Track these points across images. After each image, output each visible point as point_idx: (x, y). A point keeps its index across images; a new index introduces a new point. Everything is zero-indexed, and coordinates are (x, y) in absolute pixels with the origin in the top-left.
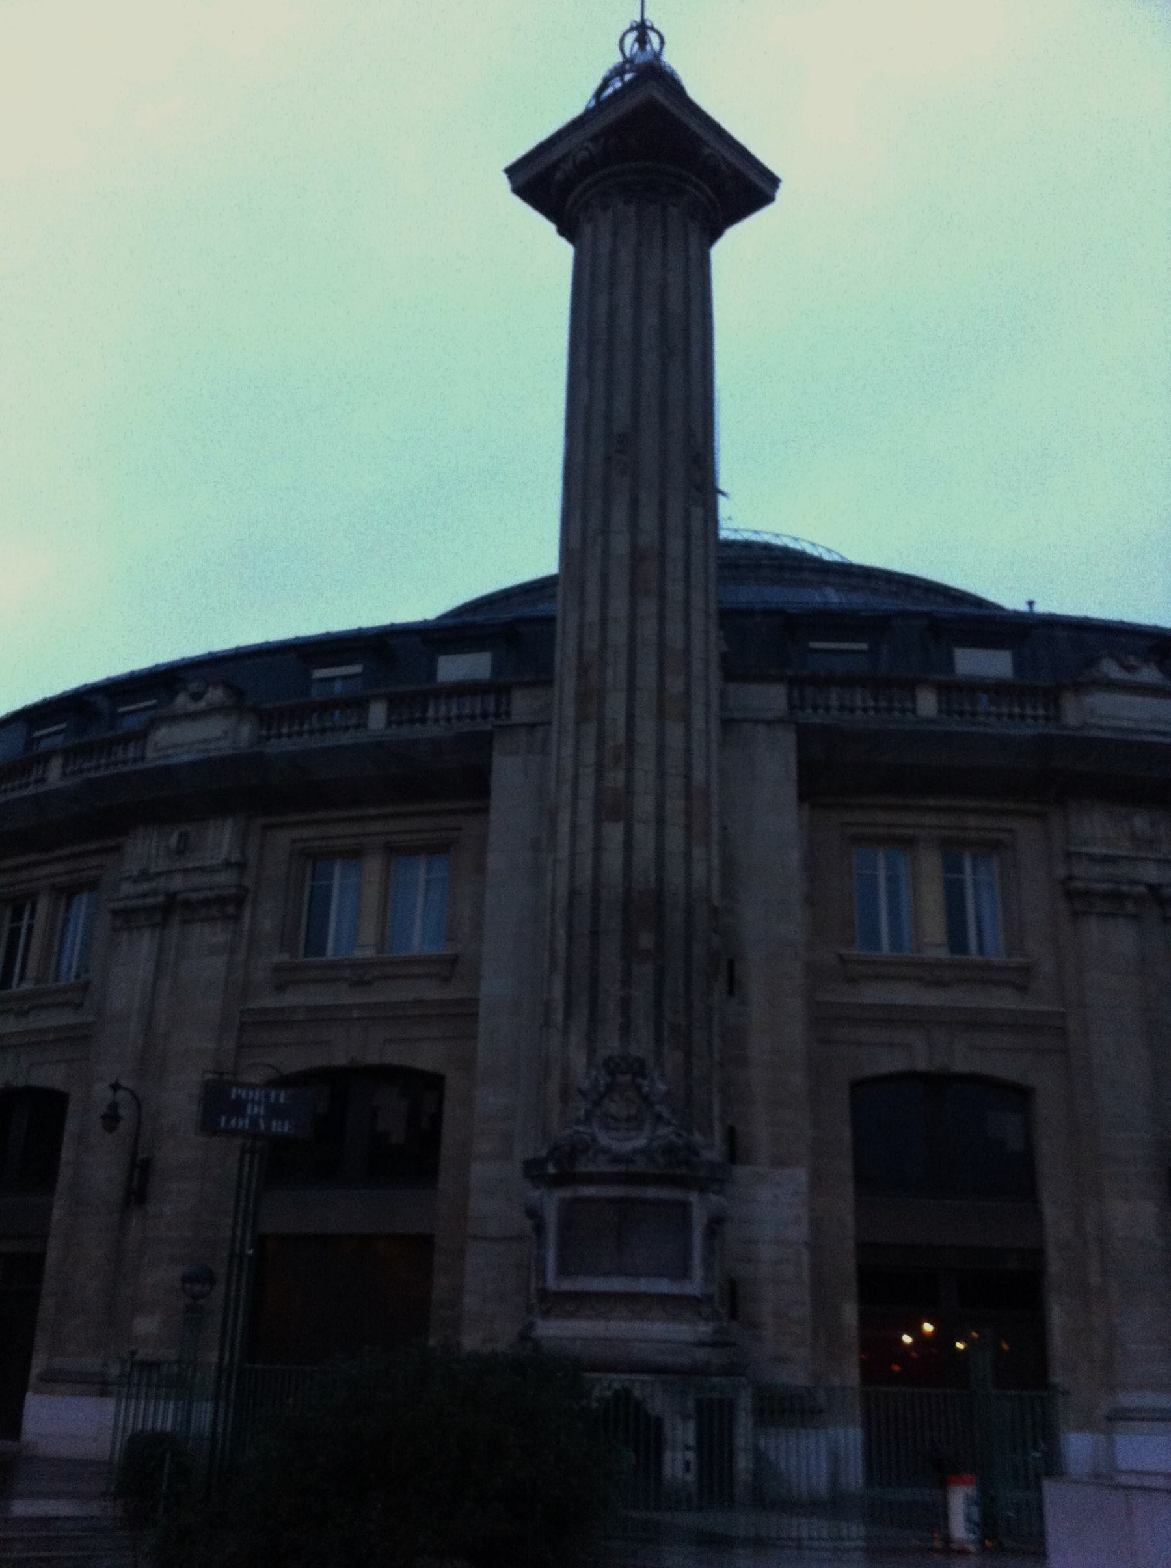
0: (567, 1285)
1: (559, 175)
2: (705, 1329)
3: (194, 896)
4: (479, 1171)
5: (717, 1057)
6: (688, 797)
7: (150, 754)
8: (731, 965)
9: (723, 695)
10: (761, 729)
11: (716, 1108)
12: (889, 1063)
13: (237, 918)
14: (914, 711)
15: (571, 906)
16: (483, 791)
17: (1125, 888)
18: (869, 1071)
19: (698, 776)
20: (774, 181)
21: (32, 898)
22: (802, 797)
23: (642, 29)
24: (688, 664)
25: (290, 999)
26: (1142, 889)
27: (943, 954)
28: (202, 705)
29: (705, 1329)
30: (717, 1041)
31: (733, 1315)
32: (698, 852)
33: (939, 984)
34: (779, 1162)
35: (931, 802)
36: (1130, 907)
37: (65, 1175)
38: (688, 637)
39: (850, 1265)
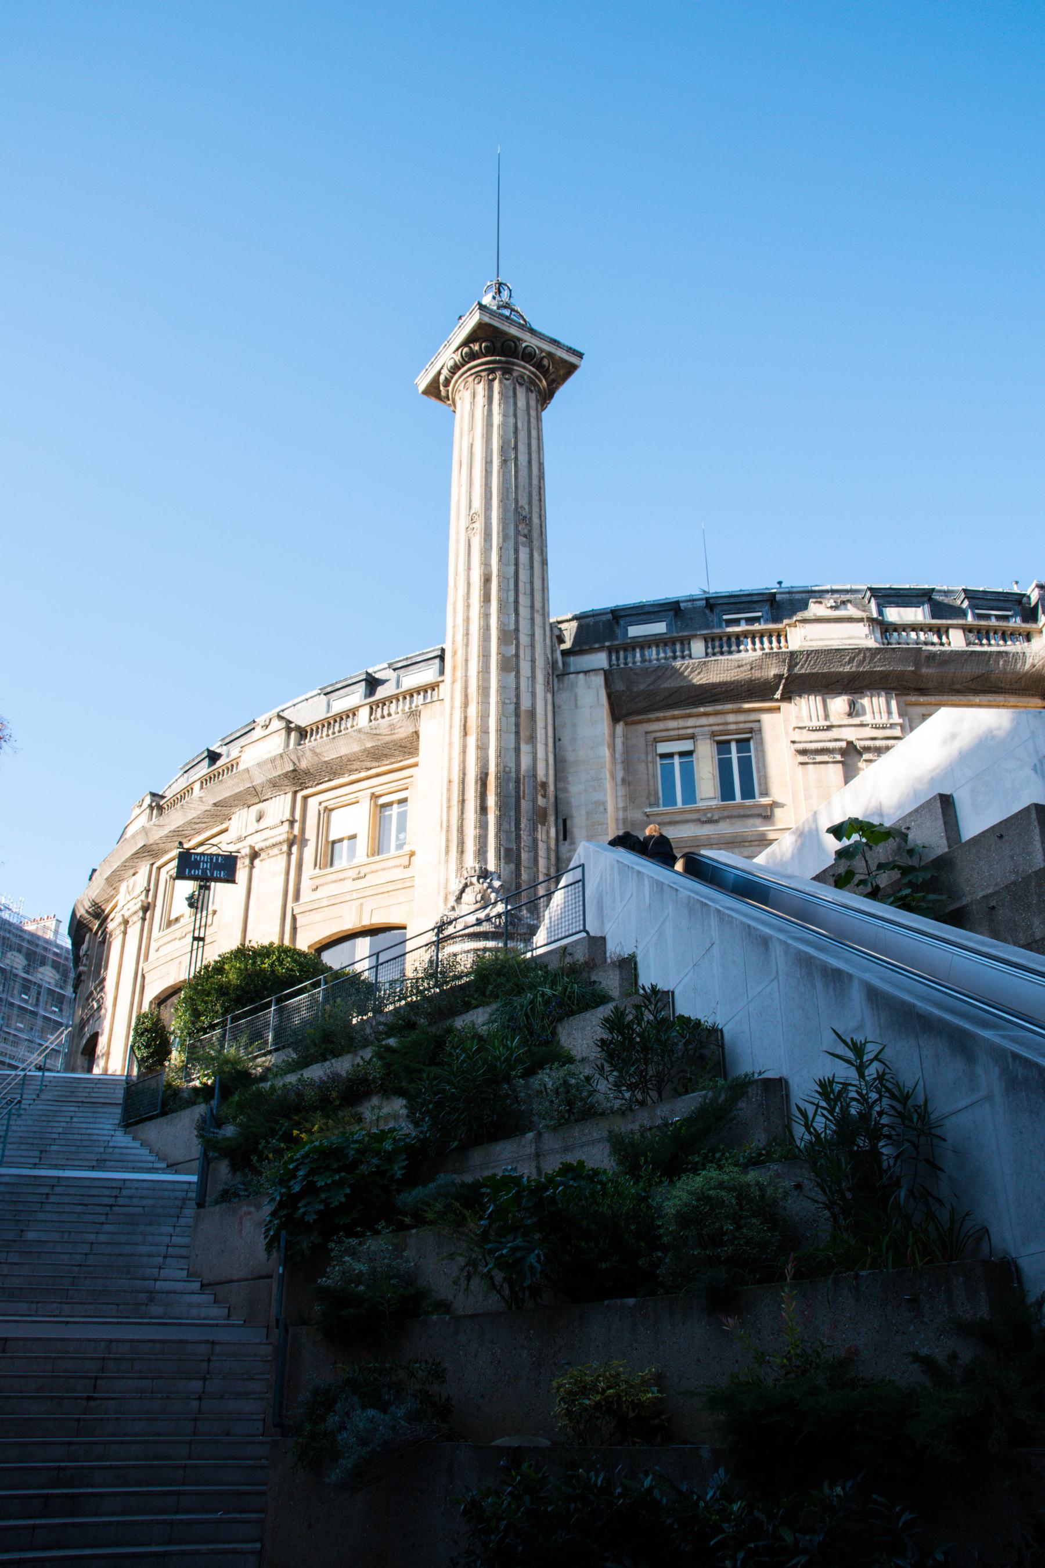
6: (517, 715)
8: (565, 821)
10: (581, 676)
13: (289, 854)
15: (449, 790)
19: (525, 704)
22: (616, 717)
24: (517, 639)
26: (844, 744)
28: (268, 731)
33: (710, 821)
35: (702, 710)
36: (839, 758)
38: (517, 621)
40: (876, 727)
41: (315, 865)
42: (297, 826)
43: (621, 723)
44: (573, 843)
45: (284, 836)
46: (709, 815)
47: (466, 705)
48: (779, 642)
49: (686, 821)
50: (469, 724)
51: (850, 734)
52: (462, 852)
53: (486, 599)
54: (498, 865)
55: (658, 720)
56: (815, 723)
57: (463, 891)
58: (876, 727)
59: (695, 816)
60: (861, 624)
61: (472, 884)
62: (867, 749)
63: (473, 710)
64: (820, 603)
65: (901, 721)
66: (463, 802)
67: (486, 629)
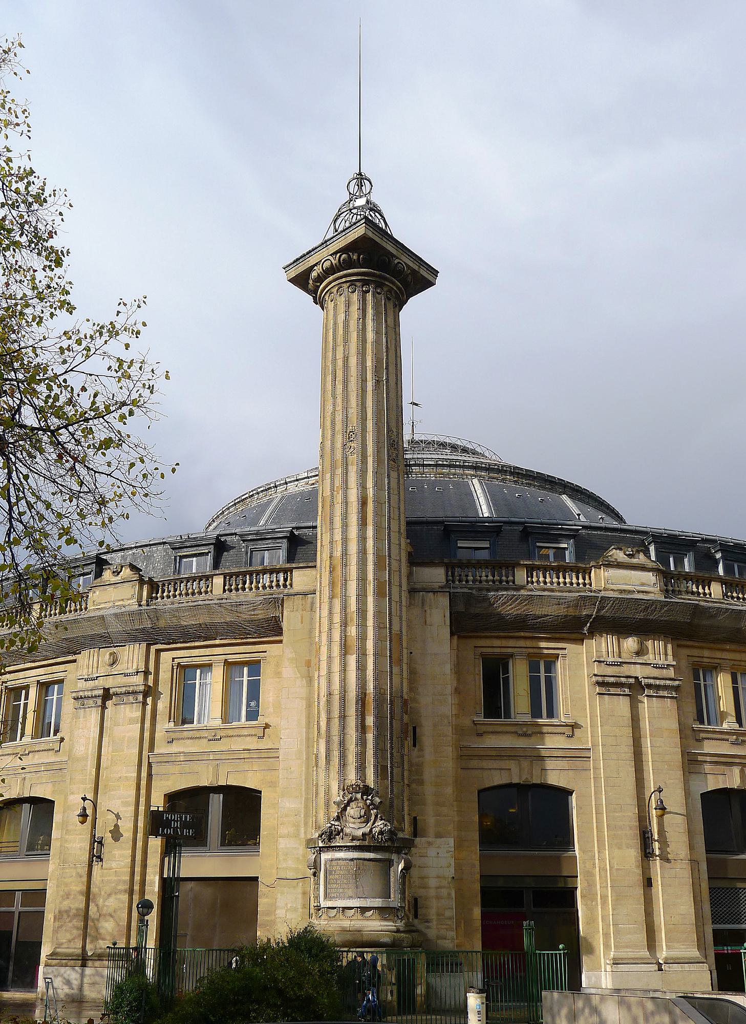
0: (330, 904)
1: (314, 274)
2: (400, 924)
3: (119, 690)
4: (283, 843)
5: (406, 782)
7: (90, 607)
8: (414, 728)
9: (410, 575)
10: (431, 594)
11: (406, 809)
12: (498, 779)
14: (514, 582)
15: (329, 702)
16: (279, 631)
17: (623, 680)
18: (488, 784)
19: (396, 628)
20: (435, 273)
21: (27, 688)
22: (452, 634)
23: (361, 178)
25: (174, 748)
26: (632, 681)
27: (528, 719)
28: (118, 579)
29: (400, 924)
30: (406, 773)
31: (416, 916)
32: (396, 670)
33: (525, 735)
34: (439, 835)
35: (522, 634)
37: (54, 844)
39: (477, 886)
40: (656, 667)
41: (170, 719)
42: (151, 677)
43: (456, 637)
44: (421, 750)
45: (142, 688)
46: (525, 729)
47: (345, 624)
48: (584, 579)
49: (507, 732)
50: (349, 643)
51: (638, 671)
52: (343, 765)
53: (363, 523)
54: (376, 782)
55: (486, 637)
56: (611, 659)
57: (348, 804)
58: (656, 667)
59: (513, 729)
60: (651, 574)
61: (356, 799)
62: (649, 686)
63: (353, 631)
64: (621, 549)
65: (674, 663)
66: (343, 717)
67: (362, 552)
